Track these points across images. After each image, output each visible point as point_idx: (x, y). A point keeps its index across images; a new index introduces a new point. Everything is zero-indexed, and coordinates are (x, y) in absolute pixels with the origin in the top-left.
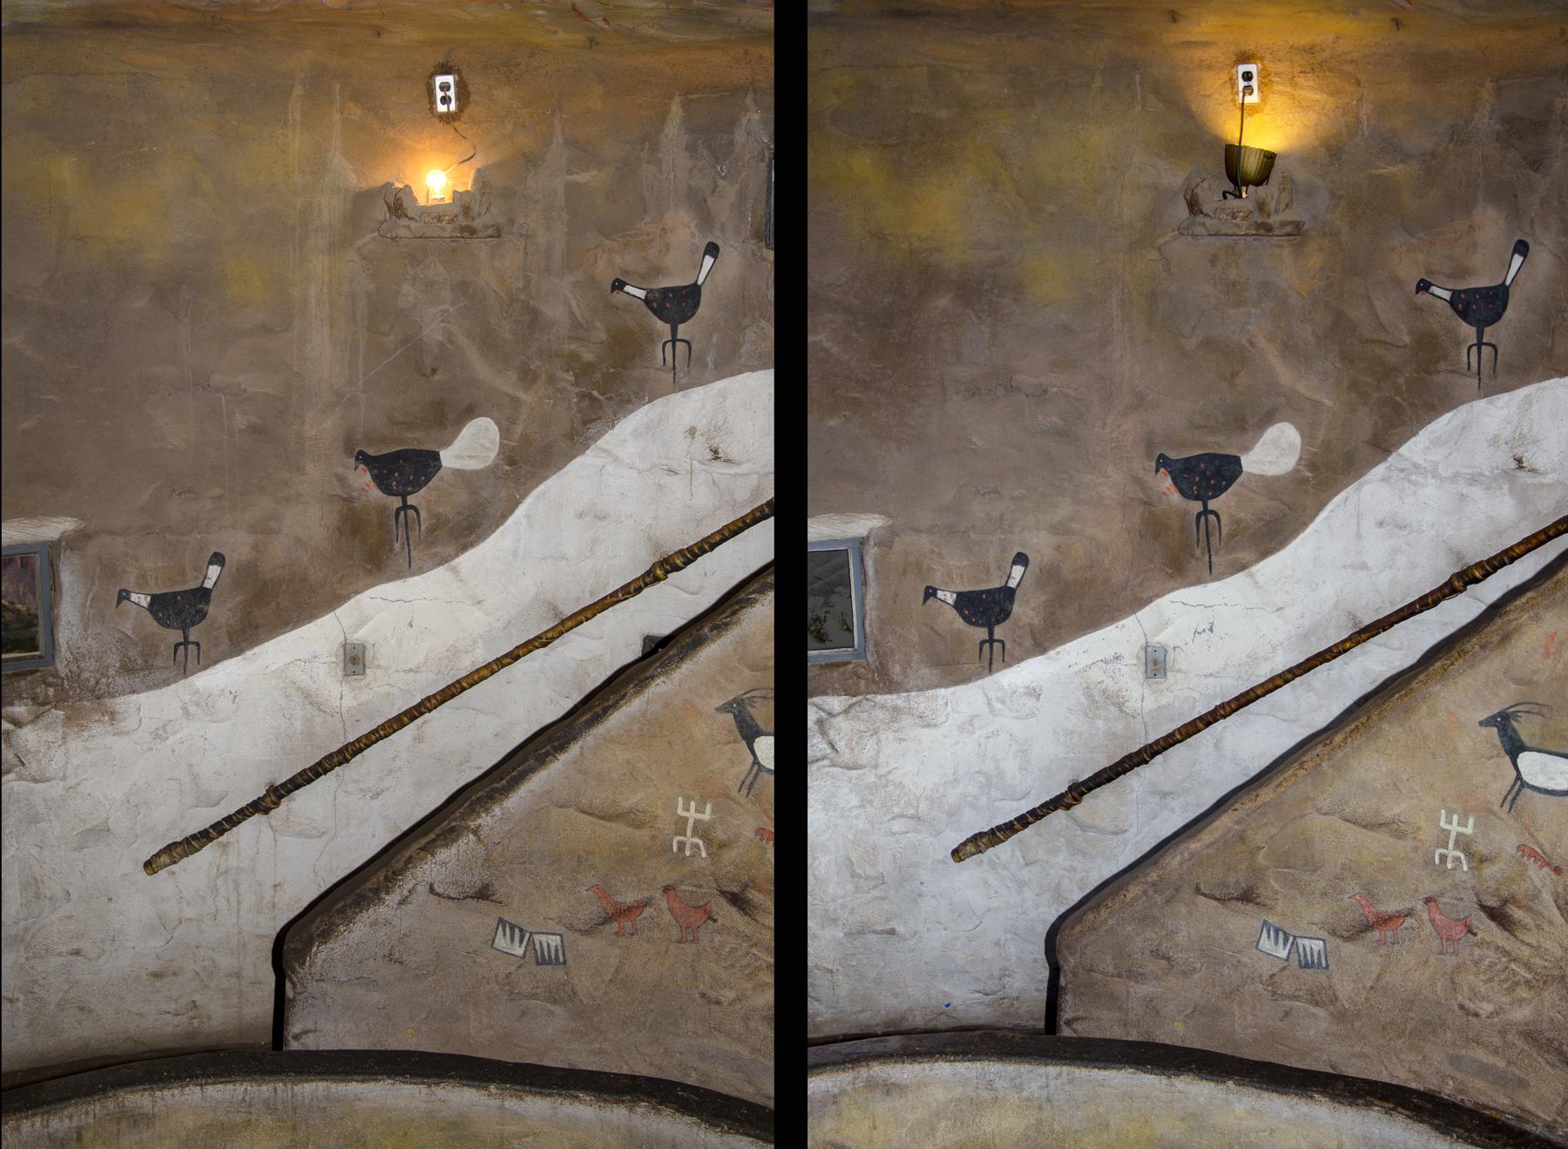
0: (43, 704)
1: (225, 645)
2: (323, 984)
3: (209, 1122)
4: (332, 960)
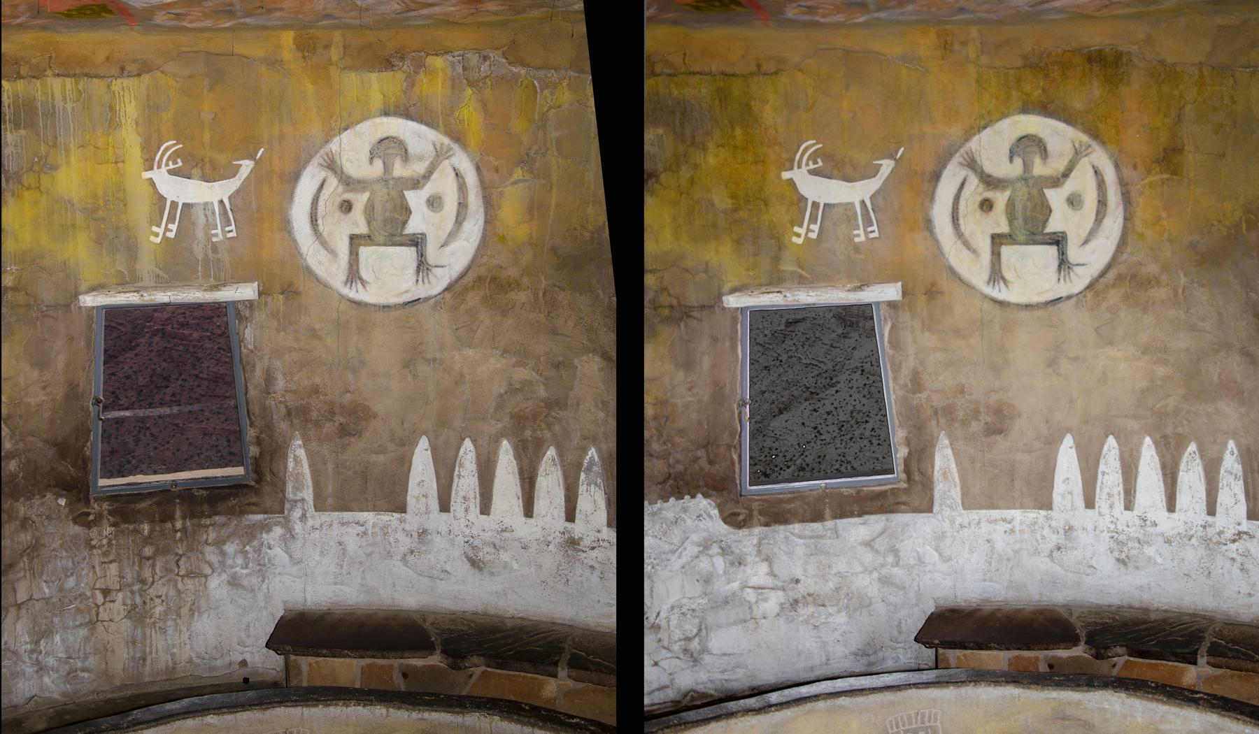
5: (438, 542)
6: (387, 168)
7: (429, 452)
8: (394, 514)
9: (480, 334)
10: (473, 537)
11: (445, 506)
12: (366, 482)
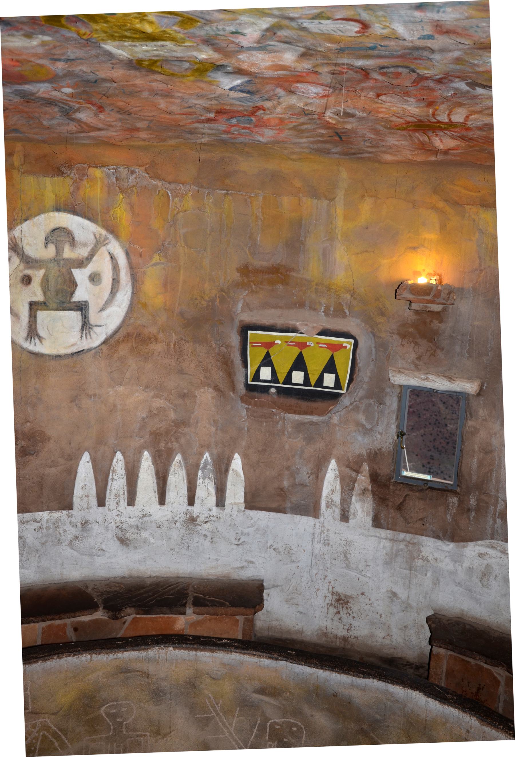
5: (96, 529)
6: (59, 251)
7: (90, 464)
8: (63, 511)
9: (128, 375)
10: (122, 523)
11: (101, 503)
12: (42, 489)
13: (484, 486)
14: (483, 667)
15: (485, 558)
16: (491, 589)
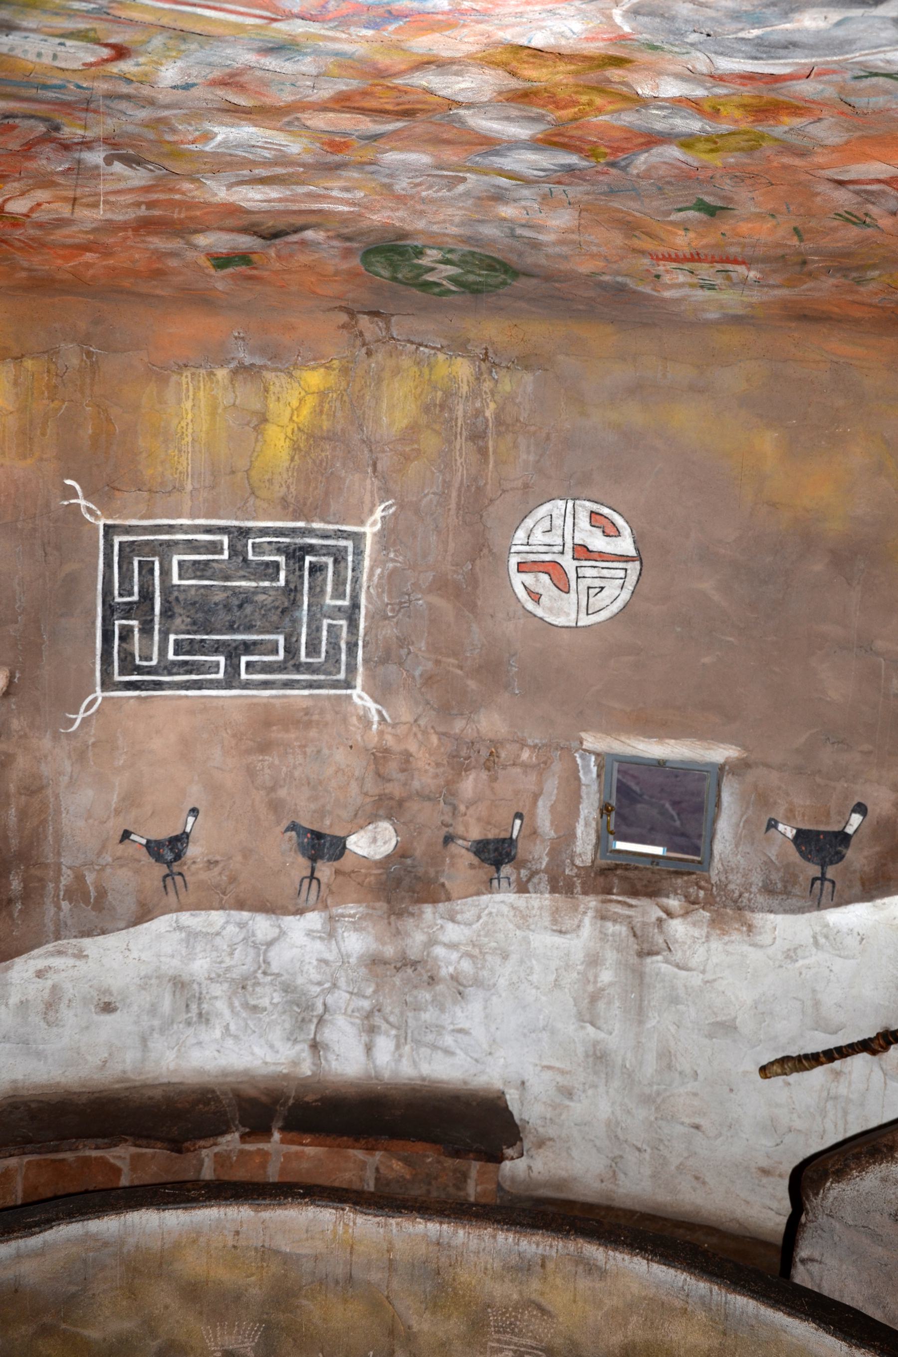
0: (694, 903)
1: (857, 889)
2: (833, 1221)
3: (651, 1296)
4: (843, 1200)
13: (34, 852)
14: (90, 1157)
15: (48, 975)
16: (63, 1026)
